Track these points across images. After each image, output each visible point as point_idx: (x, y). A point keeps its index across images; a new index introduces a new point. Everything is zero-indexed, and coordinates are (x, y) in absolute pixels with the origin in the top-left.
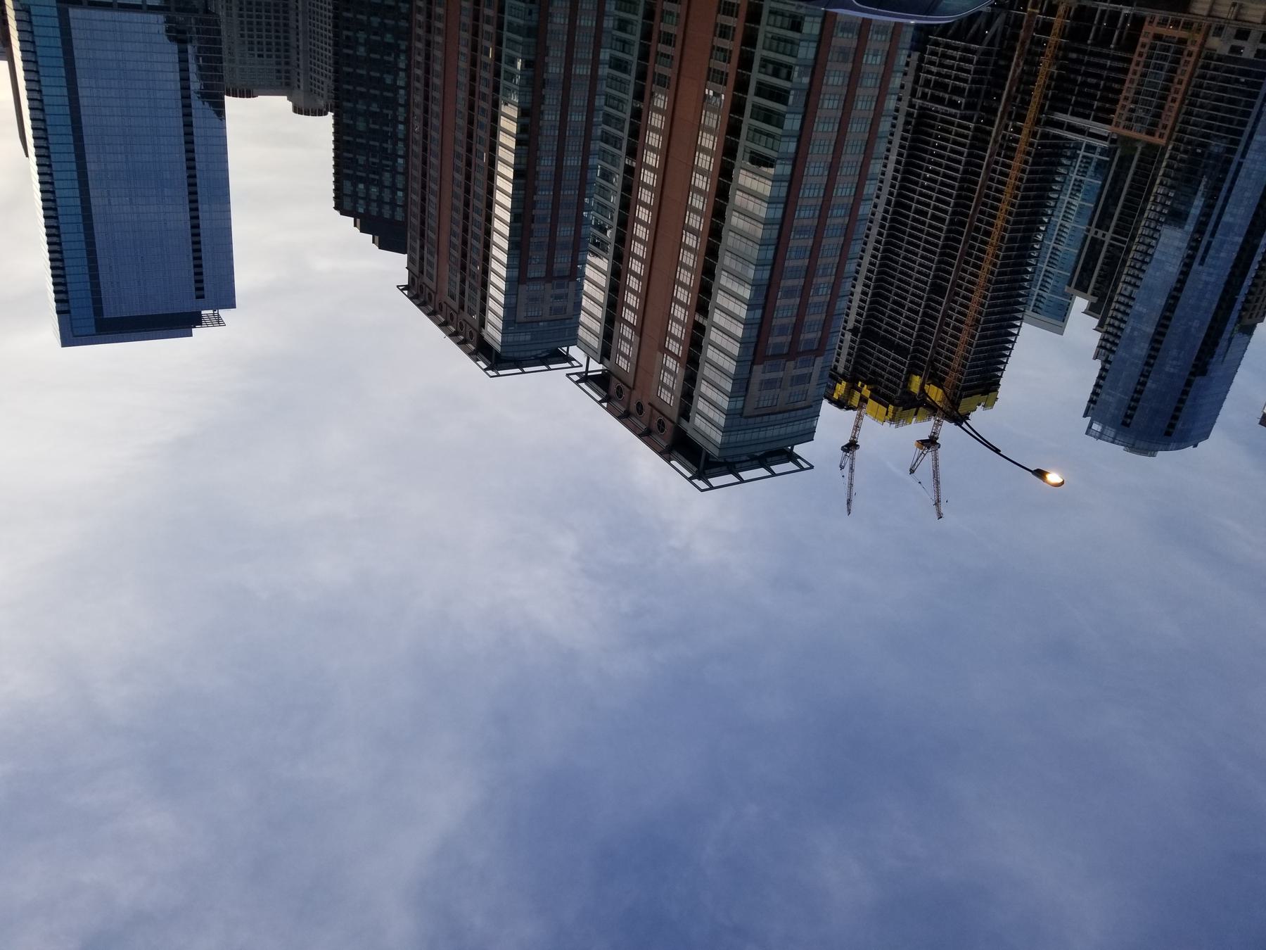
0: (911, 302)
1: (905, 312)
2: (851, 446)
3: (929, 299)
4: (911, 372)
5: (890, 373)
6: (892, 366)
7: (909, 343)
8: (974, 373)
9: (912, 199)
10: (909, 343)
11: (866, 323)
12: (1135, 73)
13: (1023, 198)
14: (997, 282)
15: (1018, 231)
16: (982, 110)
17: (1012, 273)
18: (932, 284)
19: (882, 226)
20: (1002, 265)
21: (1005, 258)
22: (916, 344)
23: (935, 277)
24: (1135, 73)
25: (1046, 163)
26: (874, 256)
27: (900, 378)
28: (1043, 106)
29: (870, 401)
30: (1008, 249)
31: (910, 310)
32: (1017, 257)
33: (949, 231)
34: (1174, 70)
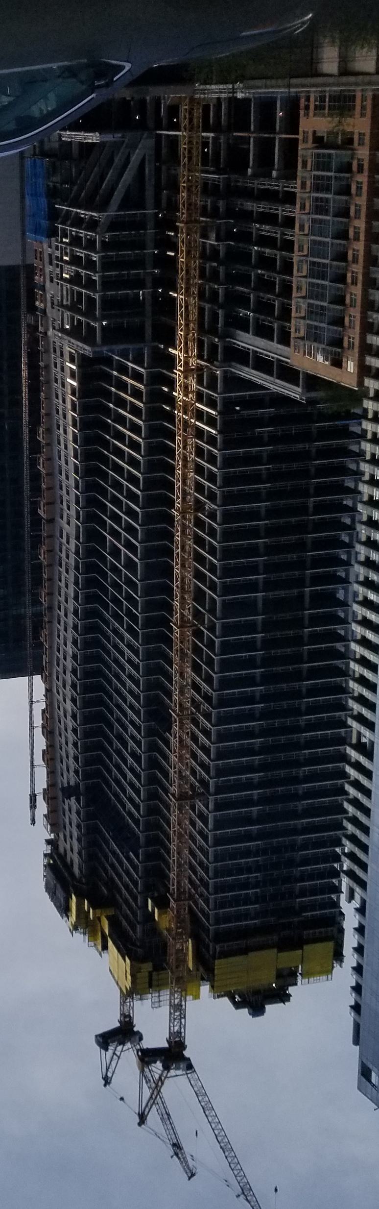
0: (133, 737)
1: (130, 760)
2: (125, 1032)
3: (150, 732)
4: (149, 889)
5: (127, 887)
6: (128, 873)
7: (137, 822)
8: (236, 901)
9: (103, 524)
10: (137, 822)
11: (87, 776)
12: (302, 228)
13: (228, 517)
14: (223, 702)
15: (253, 587)
16: (157, 337)
17: (266, 679)
18: (149, 701)
19: (76, 583)
20: (226, 665)
21: (226, 647)
22: (148, 826)
23: (149, 686)
24: (302, 228)
25: (273, 439)
26: (75, 642)
27: (135, 899)
28: (215, 317)
29: (110, 943)
30: (227, 630)
31: (134, 755)
32: (267, 644)
33: (147, 591)
34: (344, 213)
